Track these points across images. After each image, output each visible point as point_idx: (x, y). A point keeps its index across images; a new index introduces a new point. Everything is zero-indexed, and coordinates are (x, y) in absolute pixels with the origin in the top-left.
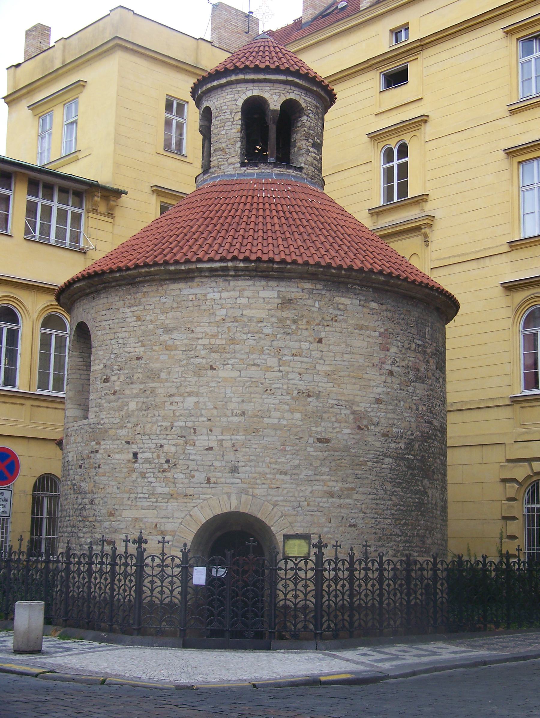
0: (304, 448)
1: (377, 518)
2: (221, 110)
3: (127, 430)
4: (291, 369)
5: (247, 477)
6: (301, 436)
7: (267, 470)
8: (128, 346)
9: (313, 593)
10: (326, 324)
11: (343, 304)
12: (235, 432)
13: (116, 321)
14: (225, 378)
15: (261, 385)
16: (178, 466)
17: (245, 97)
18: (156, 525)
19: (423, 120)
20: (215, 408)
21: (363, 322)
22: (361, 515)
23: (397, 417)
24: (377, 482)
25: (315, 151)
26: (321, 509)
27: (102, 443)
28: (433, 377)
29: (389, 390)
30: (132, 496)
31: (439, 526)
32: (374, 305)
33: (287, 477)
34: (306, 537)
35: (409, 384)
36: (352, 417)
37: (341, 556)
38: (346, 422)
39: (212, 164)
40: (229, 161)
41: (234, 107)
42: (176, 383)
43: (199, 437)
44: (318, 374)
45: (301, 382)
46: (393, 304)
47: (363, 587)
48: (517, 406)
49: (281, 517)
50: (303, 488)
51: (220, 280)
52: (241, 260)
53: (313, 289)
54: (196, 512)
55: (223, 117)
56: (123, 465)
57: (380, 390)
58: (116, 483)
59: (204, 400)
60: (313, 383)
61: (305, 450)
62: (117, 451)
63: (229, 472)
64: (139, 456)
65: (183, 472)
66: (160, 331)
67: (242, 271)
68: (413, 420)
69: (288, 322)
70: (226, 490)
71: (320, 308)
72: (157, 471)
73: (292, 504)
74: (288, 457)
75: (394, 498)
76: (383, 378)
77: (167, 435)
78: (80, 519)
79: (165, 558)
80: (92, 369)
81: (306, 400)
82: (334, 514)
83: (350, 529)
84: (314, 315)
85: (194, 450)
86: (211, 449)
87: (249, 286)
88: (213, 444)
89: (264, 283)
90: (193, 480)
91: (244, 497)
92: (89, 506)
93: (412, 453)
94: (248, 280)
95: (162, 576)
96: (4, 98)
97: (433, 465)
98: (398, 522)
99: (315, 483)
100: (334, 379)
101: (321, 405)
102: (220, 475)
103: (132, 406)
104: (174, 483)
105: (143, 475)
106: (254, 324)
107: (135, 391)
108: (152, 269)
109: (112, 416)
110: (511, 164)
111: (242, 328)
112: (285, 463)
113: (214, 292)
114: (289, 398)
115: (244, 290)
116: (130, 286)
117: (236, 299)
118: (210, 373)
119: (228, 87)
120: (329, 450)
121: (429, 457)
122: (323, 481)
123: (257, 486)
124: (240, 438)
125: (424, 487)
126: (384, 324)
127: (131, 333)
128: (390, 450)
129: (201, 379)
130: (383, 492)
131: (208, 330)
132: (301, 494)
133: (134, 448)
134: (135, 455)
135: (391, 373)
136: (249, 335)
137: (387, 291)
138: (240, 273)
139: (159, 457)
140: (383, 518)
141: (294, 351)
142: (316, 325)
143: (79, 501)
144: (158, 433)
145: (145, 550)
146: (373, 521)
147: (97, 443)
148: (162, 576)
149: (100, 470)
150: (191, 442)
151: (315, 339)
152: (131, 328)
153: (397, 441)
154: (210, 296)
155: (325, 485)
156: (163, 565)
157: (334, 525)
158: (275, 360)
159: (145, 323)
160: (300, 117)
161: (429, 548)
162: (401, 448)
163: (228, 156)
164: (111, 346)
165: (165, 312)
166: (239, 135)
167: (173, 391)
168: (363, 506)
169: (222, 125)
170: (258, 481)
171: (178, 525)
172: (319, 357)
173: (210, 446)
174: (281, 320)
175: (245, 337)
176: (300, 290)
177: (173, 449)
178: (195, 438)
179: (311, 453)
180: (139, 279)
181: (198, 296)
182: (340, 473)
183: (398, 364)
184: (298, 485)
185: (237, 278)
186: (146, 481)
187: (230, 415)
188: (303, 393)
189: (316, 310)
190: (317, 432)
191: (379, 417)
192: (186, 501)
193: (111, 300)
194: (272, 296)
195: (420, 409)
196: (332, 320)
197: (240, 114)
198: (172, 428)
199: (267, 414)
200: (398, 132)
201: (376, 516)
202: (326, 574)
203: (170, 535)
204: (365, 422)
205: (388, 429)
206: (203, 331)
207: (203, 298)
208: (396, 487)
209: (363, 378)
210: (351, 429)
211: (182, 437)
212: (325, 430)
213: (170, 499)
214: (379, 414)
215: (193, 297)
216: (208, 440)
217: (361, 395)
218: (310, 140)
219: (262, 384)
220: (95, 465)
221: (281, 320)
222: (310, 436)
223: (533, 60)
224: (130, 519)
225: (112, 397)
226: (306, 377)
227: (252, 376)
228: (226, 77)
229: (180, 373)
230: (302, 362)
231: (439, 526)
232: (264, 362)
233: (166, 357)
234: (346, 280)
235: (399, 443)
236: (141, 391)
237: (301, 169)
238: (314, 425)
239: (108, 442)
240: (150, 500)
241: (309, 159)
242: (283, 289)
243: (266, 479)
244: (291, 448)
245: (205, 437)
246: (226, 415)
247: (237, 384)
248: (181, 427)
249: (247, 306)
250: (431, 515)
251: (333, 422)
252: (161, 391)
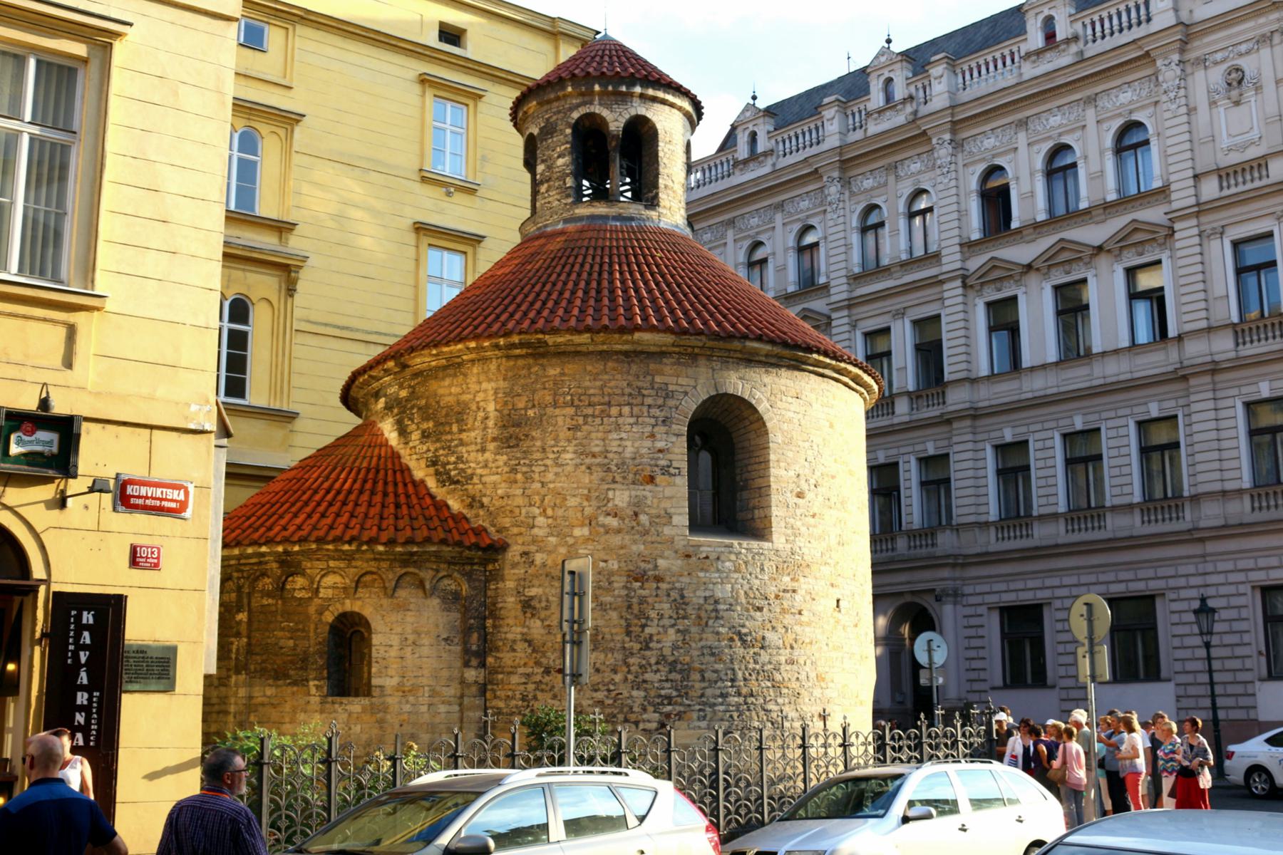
27: (802, 579)
78: (769, 684)
200: (250, 114)
220: (793, 610)
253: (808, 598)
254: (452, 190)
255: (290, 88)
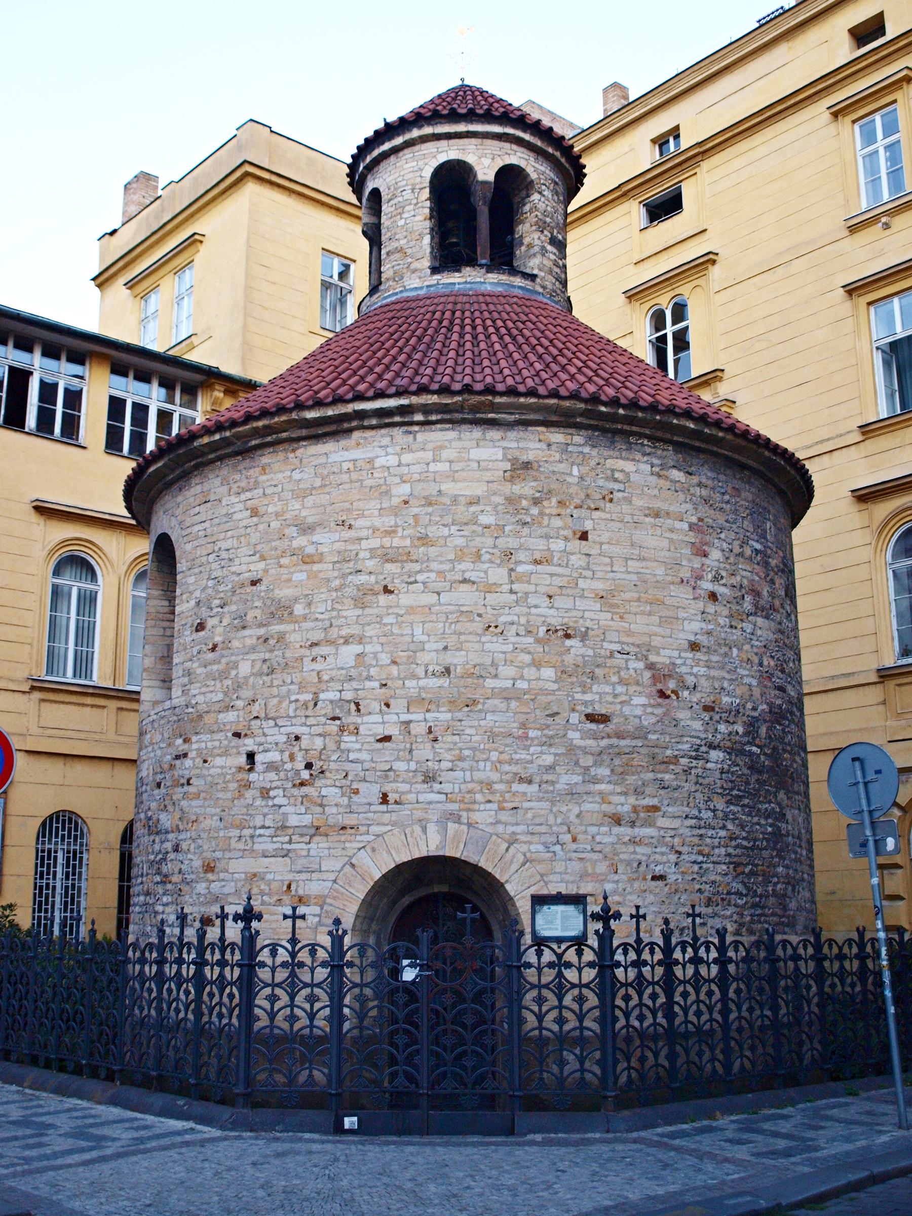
0: (561, 733)
1: (702, 862)
2: (396, 189)
3: (235, 713)
4: (532, 588)
5: (457, 791)
6: (555, 709)
7: (495, 776)
8: (237, 561)
9: (597, 1013)
10: (593, 506)
11: (622, 471)
12: (432, 707)
13: (217, 521)
14: (412, 607)
15: (478, 619)
16: (327, 774)
17: (435, 163)
18: (289, 886)
19: (709, 260)
20: (394, 662)
21: (658, 504)
22: (673, 857)
23: (727, 676)
24: (699, 795)
25: (555, 250)
26: (598, 847)
27: (194, 739)
28: (781, 610)
29: (710, 627)
30: (247, 832)
31: (806, 876)
32: (676, 474)
33: (534, 788)
34: (578, 900)
35: (745, 617)
36: (647, 674)
37: (645, 938)
38: (638, 684)
39: (384, 276)
40: (413, 266)
41: (418, 179)
42: (323, 620)
43: (366, 719)
44: (582, 597)
45: (552, 612)
46: (709, 474)
47: (692, 997)
48: (891, 684)
49: (524, 864)
50: (564, 809)
51: (397, 432)
52: (433, 392)
53: (568, 444)
54: (364, 859)
55: (400, 199)
56: (228, 777)
57: (696, 626)
58: (218, 810)
59: (373, 650)
60: (574, 613)
61: (565, 735)
62: (219, 752)
63: (424, 782)
64: (258, 758)
65: (337, 784)
66: (292, 531)
67: (438, 412)
68: (754, 682)
69: (524, 503)
70: (418, 814)
71: (582, 478)
72: (290, 785)
73: (544, 839)
74: (532, 750)
75: (730, 826)
76: (700, 605)
77: (307, 717)
79: (297, 948)
80: (178, 610)
81: (563, 643)
82: (622, 856)
83: (653, 883)
84: (571, 491)
85: (357, 741)
86: (387, 739)
87: (450, 441)
88: (393, 731)
89: (477, 433)
90: (355, 798)
91: (452, 827)
92: (172, 856)
93: (757, 741)
94: (447, 429)
95: (293, 984)
96: (94, 279)
97: (791, 766)
98: (739, 870)
99: (585, 797)
100: (613, 606)
101: (590, 652)
102: (404, 787)
103: (245, 668)
104: (321, 805)
105: (265, 793)
106: (461, 508)
107: (249, 642)
108: (276, 419)
109: (211, 689)
110: (856, 307)
111: (441, 516)
112: (527, 762)
113: (387, 454)
114: (531, 640)
115: (442, 447)
116: (240, 458)
117: (428, 464)
118: (383, 599)
119: (406, 151)
120: (609, 737)
121: (785, 751)
122: (600, 793)
123: (476, 807)
124: (444, 716)
125: (779, 804)
126: (696, 509)
127: (242, 539)
128: (719, 736)
129: (367, 611)
130: (710, 814)
131: (377, 522)
132: (559, 821)
133: (249, 744)
134: (251, 756)
135: (713, 596)
136: (454, 529)
137: (699, 450)
138: (434, 418)
139: (292, 758)
140: (714, 863)
141: (537, 556)
142: (576, 507)
143: (157, 847)
144: (292, 714)
145: (257, 932)
146: (696, 868)
147: (186, 741)
148: (293, 985)
149: (191, 789)
150: (352, 728)
151: (575, 533)
152: (242, 531)
153: (731, 719)
154: (379, 462)
155: (604, 803)
156: (293, 965)
157: (624, 877)
158: (503, 572)
159: (266, 519)
160: (528, 196)
161: (794, 917)
162: (737, 733)
163: (410, 260)
164: (208, 567)
165: (302, 495)
166: (428, 224)
167: (317, 636)
168: (676, 840)
169: (400, 210)
170: (479, 797)
171: (330, 884)
172: (584, 565)
173: (387, 733)
174: (510, 500)
175: (446, 531)
176: (544, 446)
177: (319, 743)
178: (359, 720)
179: (575, 742)
180: (253, 443)
181: (358, 464)
182: (631, 779)
183: (724, 581)
184: (553, 803)
185: (427, 427)
186: (270, 803)
187: (422, 675)
188: (556, 631)
189: (576, 480)
190: (585, 703)
191: (696, 676)
192: (343, 838)
193: (206, 486)
194: (493, 458)
195: (765, 663)
196: (604, 498)
197: (427, 190)
198: (316, 704)
199: (492, 670)
200: (671, 285)
201: (700, 858)
202: (619, 972)
203: (316, 904)
204: (672, 684)
205: (712, 698)
206: (368, 524)
207: (368, 466)
208: (732, 804)
209: (663, 603)
210: (649, 696)
211: (334, 719)
212: (600, 698)
213: (314, 835)
214: (695, 670)
215: (351, 465)
216: (383, 723)
217: (663, 633)
218: (546, 232)
219: (480, 615)
221: (510, 500)
222: (573, 710)
223: (881, 151)
224: (243, 876)
225: (211, 656)
226: (559, 602)
227: (461, 602)
228: (404, 133)
229: (329, 602)
230: (552, 575)
231: (806, 876)
232: (482, 575)
233: (303, 576)
234: (626, 427)
235: (734, 723)
236: (261, 640)
237: (533, 277)
238: (579, 689)
239: (204, 737)
240: (278, 839)
241: (546, 262)
242: (514, 445)
243: (493, 793)
244: (539, 733)
245: (377, 718)
246: (414, 676)
247: (434, 617)
248: (331, 702)
249: (447, 477)
250: (793, 856)
251: (614, 684)
252: (295, 638)
253: (199, 761)
254: (884, 220)
255: (705, 230)
